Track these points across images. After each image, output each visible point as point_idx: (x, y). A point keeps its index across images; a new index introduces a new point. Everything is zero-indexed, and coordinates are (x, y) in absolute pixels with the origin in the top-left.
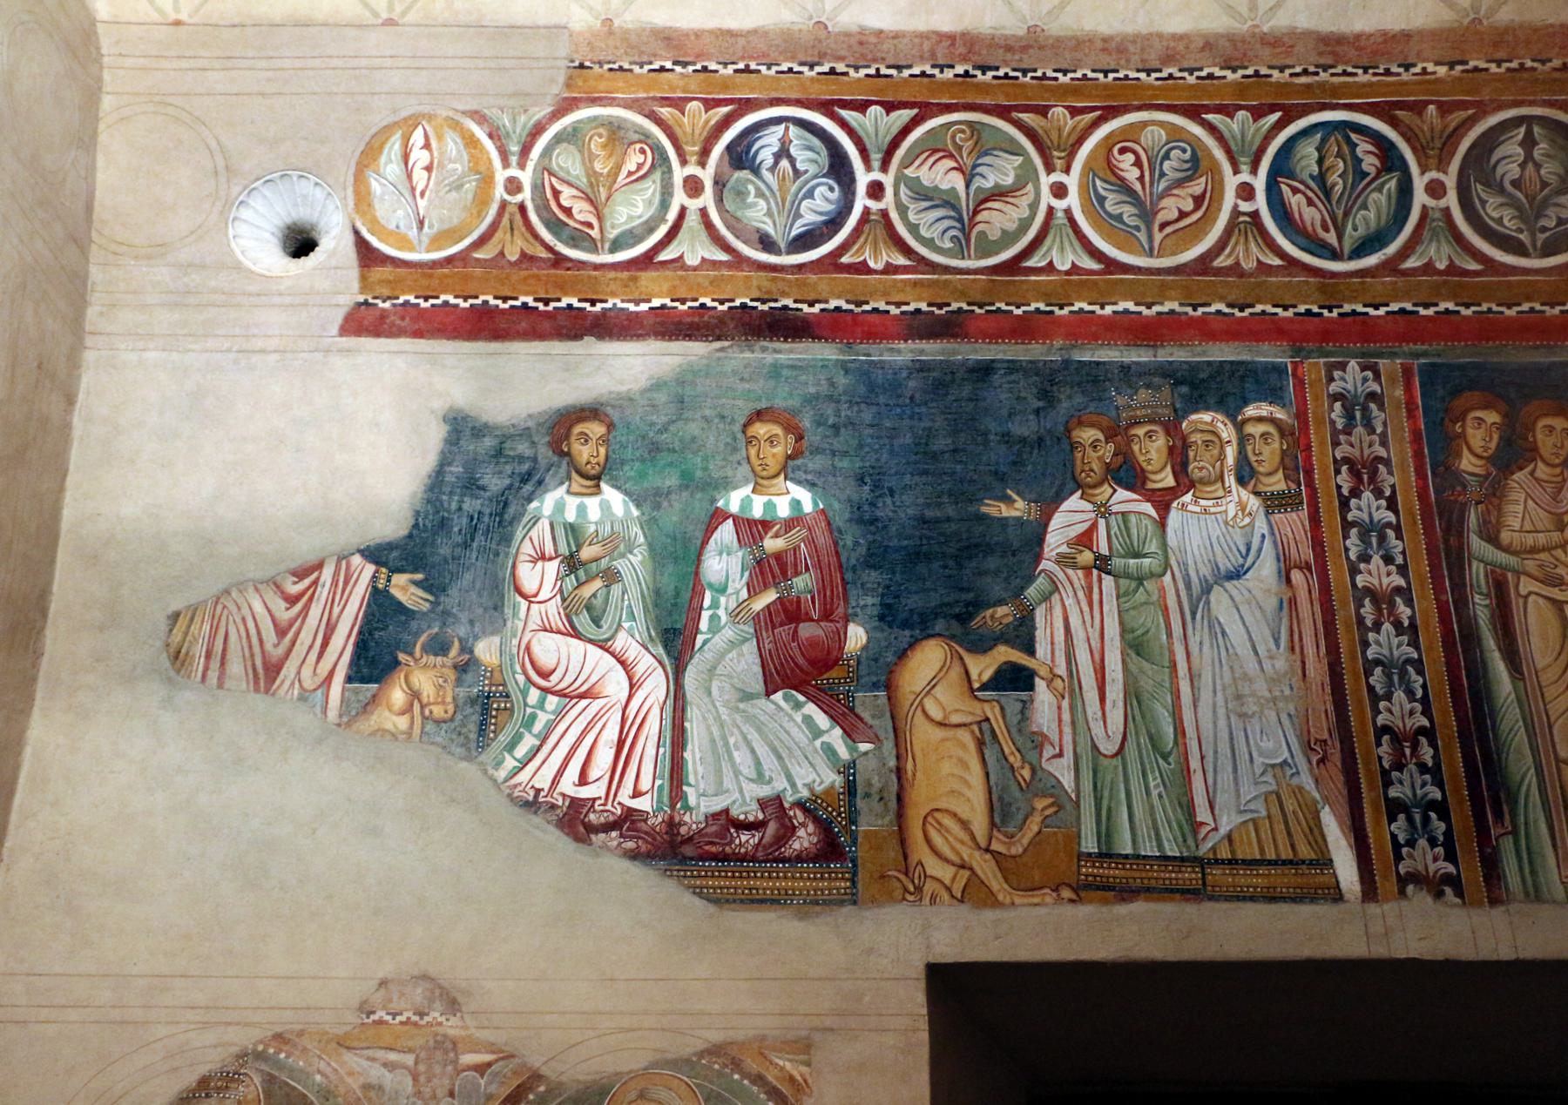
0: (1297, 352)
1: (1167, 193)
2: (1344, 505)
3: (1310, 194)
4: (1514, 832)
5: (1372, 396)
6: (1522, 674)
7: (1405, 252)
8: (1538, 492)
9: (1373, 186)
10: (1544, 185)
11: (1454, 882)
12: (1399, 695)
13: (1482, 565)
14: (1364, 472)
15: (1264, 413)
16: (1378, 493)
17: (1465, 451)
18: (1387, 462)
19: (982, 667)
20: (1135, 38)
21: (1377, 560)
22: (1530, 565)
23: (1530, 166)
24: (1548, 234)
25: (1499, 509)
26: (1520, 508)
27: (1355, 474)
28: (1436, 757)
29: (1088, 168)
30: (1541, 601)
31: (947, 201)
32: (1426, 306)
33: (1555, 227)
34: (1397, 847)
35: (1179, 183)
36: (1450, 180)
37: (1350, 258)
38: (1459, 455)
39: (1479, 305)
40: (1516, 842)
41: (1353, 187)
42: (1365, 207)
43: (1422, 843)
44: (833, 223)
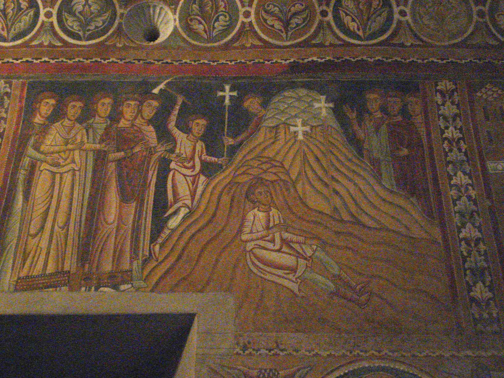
5: (7, 94)
6: (28, 201)
7: (32, 40)
8: (63, 131)
9: (24, 13)
10: (92, 13)
13: (28, 159)
17: (38, 114)
18: (5, 119)
22: (49, 159)
23: (87, 6)
24: (90, 32)
26: (52, 137)
30: (47, 172)
32: (37, 59)
33: (94, 29)
36: (55, 12)
37: (11, 41)
38: (35, 115)
39: (58, 59)
41: (17, 14)
42: (20, 22)
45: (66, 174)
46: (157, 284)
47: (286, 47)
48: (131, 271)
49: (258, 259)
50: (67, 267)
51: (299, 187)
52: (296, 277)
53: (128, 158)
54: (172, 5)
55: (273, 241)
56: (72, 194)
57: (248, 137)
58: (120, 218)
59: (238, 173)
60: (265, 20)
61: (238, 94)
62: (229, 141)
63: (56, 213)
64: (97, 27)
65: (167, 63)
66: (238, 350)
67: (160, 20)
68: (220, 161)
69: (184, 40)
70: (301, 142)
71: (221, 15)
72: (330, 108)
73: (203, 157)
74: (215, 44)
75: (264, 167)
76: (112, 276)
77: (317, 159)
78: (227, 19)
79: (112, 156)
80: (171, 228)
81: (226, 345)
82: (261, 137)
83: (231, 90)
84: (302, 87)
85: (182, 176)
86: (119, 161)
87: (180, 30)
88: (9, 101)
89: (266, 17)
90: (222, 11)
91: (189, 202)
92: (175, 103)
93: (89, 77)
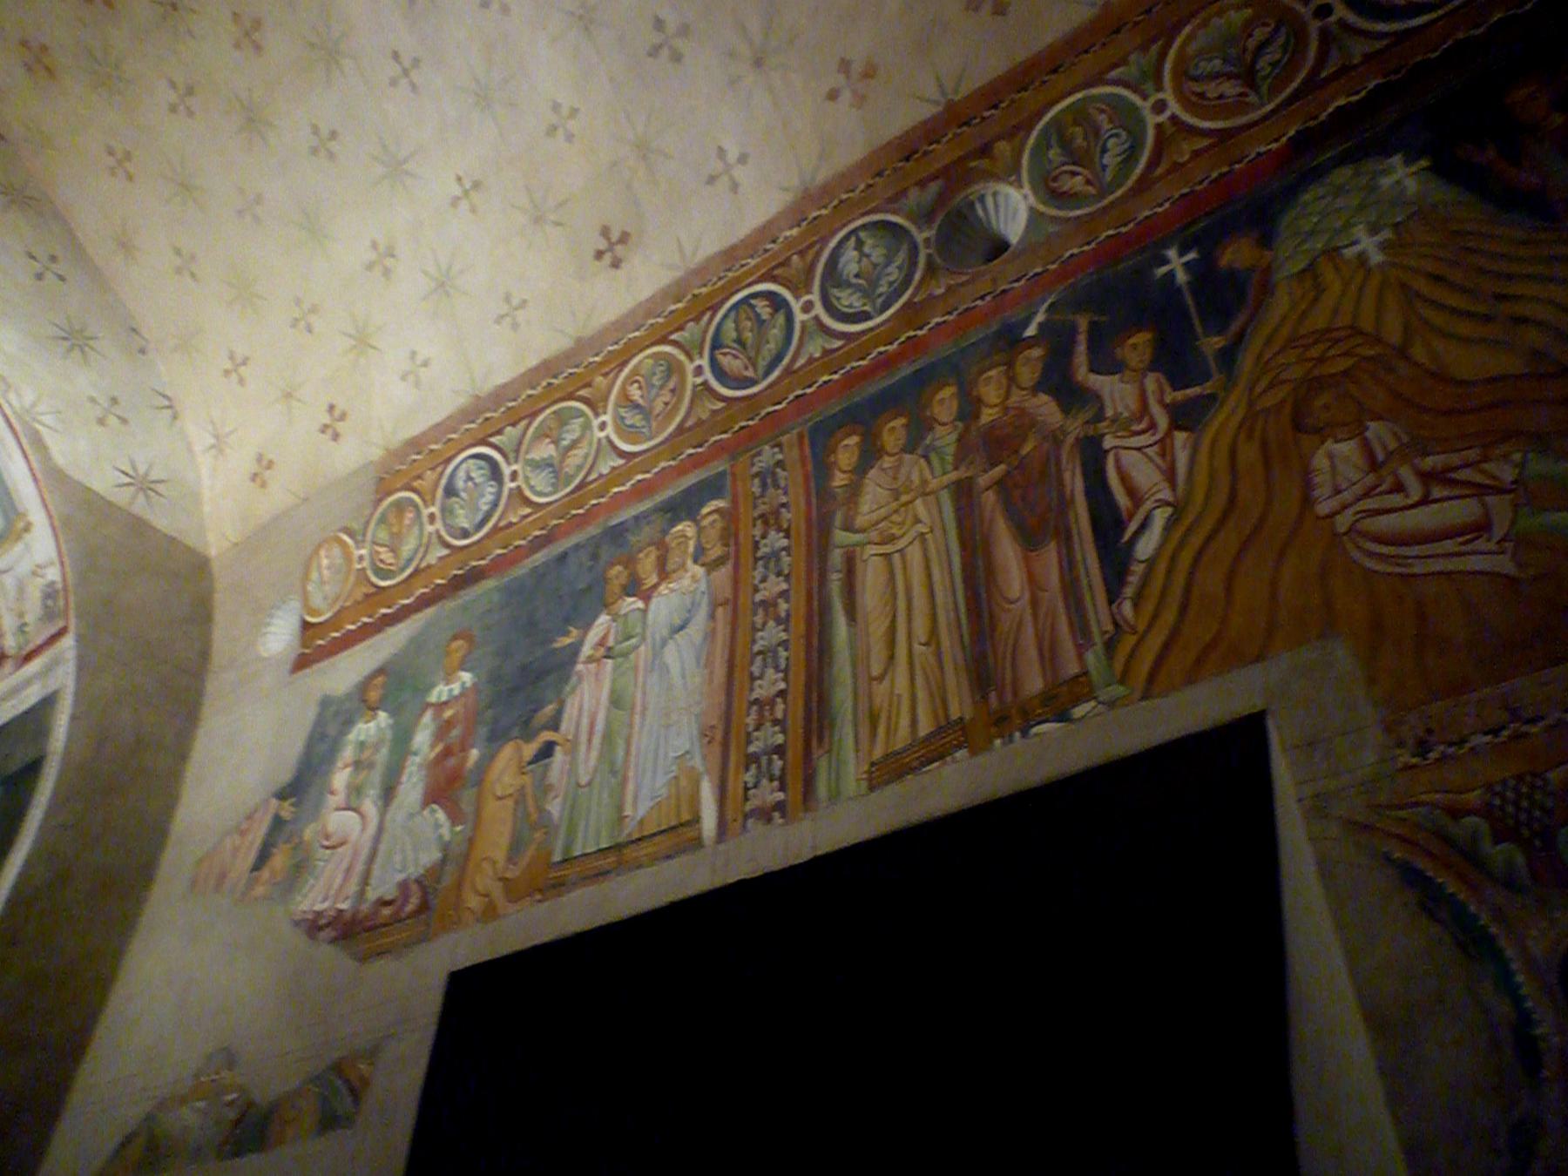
0: (733, 458)
1: (658, 395)
2: (756, 545)
3: (734, 352)
4: (829, 751)
5: (779, 464)
7: (794, 360)
10: (875, 266)
11: (780, 806)
12: (770, 672)
14: (769, 520)
15: (713, 508)
16: (779, 530)
19: (530, 750)
20: (627, 315)
21: (772, 577)
22: (874, 535)
25: (856, 503)
27: (766, 523)
28: (785, 712)
29: (618, 405)
31: (547, 464)
34: (746, 789)
35: (662, 387)
36: (815, 297)
40: (830, 762)
43: (765, 782)
44: (495, 505)
45: (910, 548)
46: (1152, 678)
47: (1266, 118)
48: (1086, 673)
49: (1378, 539)
50: (955, 713)
51: (1418, 352)
52: (1495, 540)
53: (1016, 468)
54: (1010, 176)
55: (1399, 488)
56: (929, 576)
57: (1252, 317)
58: (1032, 580)
59: (1258, 390)
60: (1202, 95)
61: (1199, 252)
62: (1213, 343)
63: (910, 620)
64: (891, 284)
65: (1036, 274)
66: (1405, 758)
67: (1002, 219)
68: (1207, 388)
69: (1054, 219)
70: (1380, 266)
71: (1111, 136)
72: (1423, 169)
73: (1168, 399)
74: (1119, 193)
75: (1315, 352)
76: (1048, 697)
77: (1438, 279)
78: (1124, 134)
79: (983, 480)
80: (1143, 558)
81: (1370, 757)
82: (1281, 303)
83: (1181, 254)
84: (1335, 167)
85: (1134, 452)
86: (1001, 485)
87: (1042, 208)
88: (785, 473)
89: (1198, 88)
90: (1108, 130)
91: (1166, 495)
92: (1073, 331)
93: (906, 370)
